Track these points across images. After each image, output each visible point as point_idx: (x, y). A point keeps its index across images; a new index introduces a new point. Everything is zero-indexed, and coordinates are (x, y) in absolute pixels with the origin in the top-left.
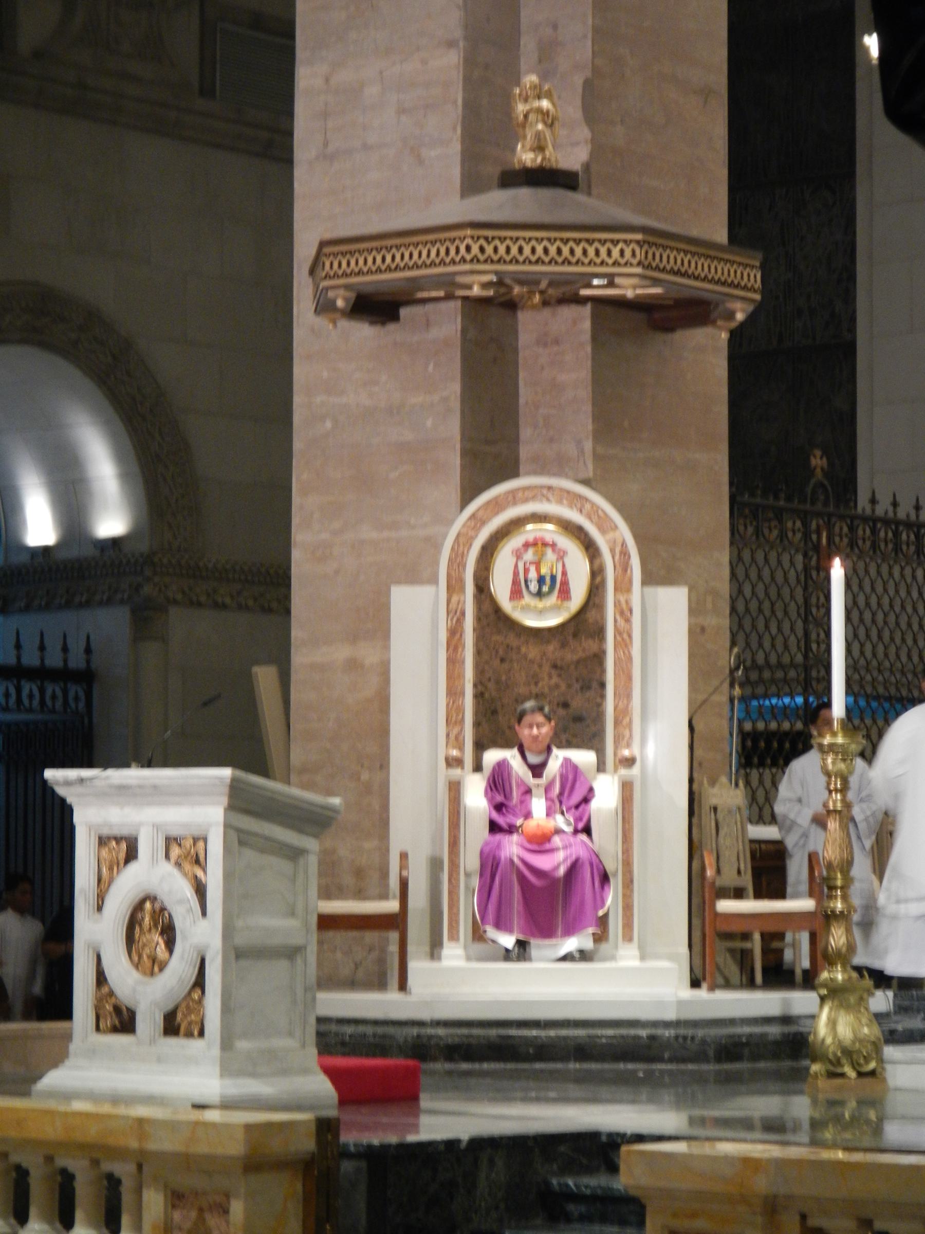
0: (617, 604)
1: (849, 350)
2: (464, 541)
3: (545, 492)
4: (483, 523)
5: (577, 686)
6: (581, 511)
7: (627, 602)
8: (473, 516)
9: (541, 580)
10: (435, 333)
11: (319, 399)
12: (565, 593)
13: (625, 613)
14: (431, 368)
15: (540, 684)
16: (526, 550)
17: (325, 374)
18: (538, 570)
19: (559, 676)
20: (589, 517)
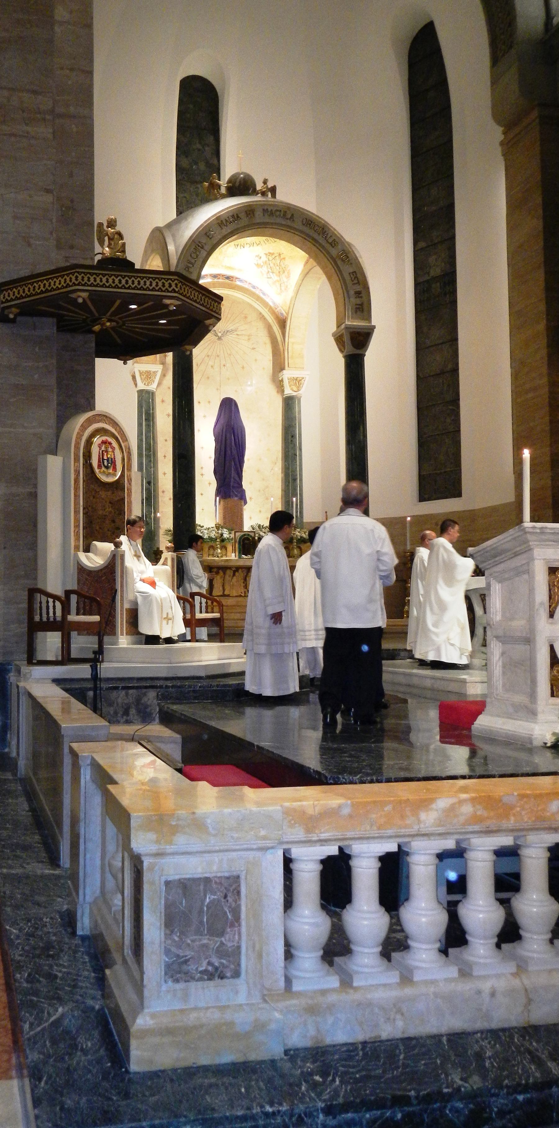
9: (108, 460)
12: (115, 469)
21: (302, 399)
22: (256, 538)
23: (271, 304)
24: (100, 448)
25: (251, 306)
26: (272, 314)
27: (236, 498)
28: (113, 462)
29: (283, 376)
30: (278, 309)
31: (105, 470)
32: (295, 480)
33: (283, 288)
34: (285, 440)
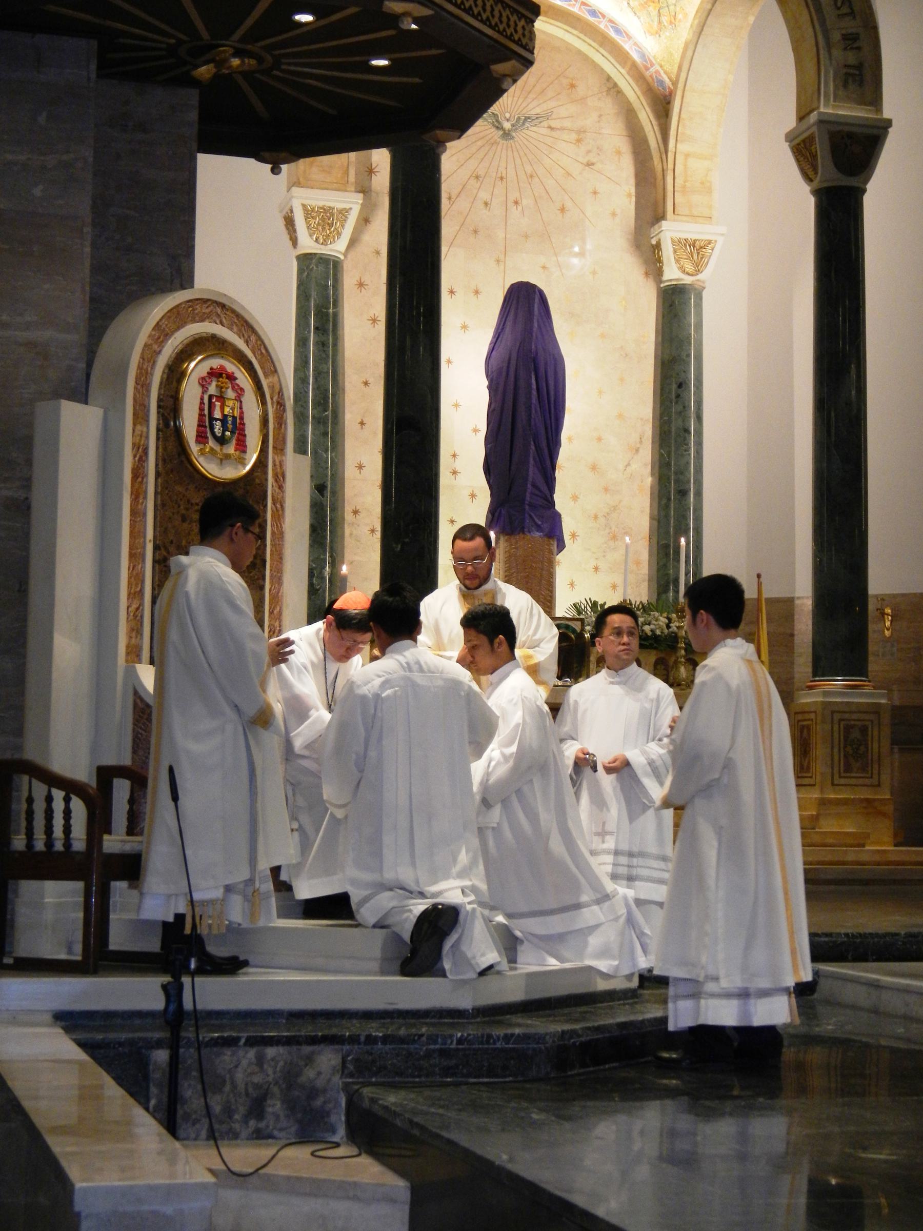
0: (274, 465)
2: (149, 356)
3: (219, 310)
4: (167, 336)
6: (247, 342)
7: (281, 466)
9: (224, 420)
12: (242, 446)
13: (280, 478)
14: (42, 119)
16: (210, 384)
20: (254, 353)
21: (704, 294)
22: (587, 635)
23: (635, 56)
24: (205, 389)
25: (586, 58)
26: (637, 82)
27: (537, 534)
28: (237, 427)
29: (662, 236)
30: (652, 70)
31: (217, 447)
32: (683, 493)
33: (665, 20)
34: (662, 389)
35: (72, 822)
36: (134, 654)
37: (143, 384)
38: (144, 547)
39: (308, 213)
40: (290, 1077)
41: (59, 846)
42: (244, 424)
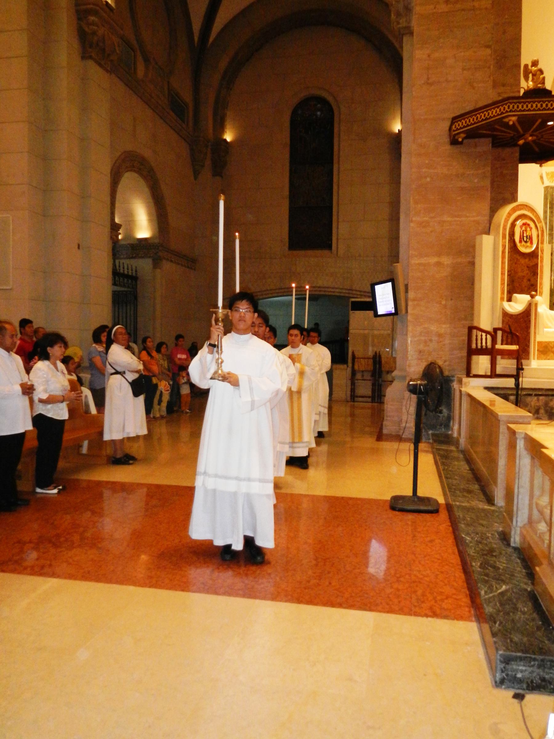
1: (331, 208)
2: (506, 221)
3: (525, 207)
5: (532, 274)
6: (533, 215)
8: (509, 213)
9: (527, 237)
10: (479, 149)
11: (424, 170)
12: (532, 243)
13: (542, 251)
14: (477, 161)
15: (524, 273)
16: (523, 227)
17: (427, 162)
18: (526, 233)
19: (529, 270)
28: (531, 238)
35: (488, 341)
36: (502, 299)
37: (505, 229)
38: (505, 271)
39: (547, 174)
40: (546, 404)
41: (484, 347)
42: (532, 237)
